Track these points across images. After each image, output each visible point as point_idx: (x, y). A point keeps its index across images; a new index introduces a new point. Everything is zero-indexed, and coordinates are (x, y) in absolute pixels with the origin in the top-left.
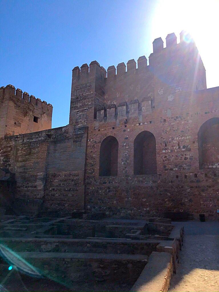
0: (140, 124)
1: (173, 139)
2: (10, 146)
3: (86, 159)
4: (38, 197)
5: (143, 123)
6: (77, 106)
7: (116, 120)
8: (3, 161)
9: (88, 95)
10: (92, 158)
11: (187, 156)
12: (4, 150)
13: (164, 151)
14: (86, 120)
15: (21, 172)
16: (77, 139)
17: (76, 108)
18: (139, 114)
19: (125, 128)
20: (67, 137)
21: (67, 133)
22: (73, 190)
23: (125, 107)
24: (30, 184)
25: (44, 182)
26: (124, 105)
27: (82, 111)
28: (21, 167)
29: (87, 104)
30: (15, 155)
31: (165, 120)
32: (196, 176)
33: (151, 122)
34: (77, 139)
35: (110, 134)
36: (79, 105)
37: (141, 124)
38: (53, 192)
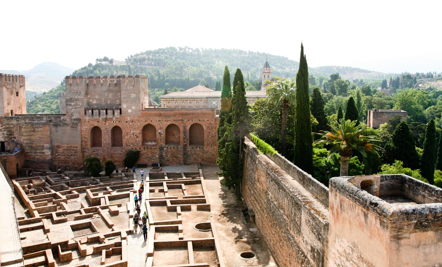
1: (130, 131)
2: (12, 124)
3: (82, 138)
4: (48, 159)
5: (116, 122)
10: (85, 138)
12: (7, 126)
15: (27, 143)
17: (70, 105)
18: (114, 116)
19: (105, 123)
20: (65, 124)
22: (74, 155)
23: (105, 111)
24: (38, 151)
25: (51, 150)
26: (104, 110)
28: (26, 140)
30: (19, 131)
31: (127, 122)
32: (140, 149)
34: (74, 126)
35: (96, 125)
36: (73, 104)
38: (59, 157)
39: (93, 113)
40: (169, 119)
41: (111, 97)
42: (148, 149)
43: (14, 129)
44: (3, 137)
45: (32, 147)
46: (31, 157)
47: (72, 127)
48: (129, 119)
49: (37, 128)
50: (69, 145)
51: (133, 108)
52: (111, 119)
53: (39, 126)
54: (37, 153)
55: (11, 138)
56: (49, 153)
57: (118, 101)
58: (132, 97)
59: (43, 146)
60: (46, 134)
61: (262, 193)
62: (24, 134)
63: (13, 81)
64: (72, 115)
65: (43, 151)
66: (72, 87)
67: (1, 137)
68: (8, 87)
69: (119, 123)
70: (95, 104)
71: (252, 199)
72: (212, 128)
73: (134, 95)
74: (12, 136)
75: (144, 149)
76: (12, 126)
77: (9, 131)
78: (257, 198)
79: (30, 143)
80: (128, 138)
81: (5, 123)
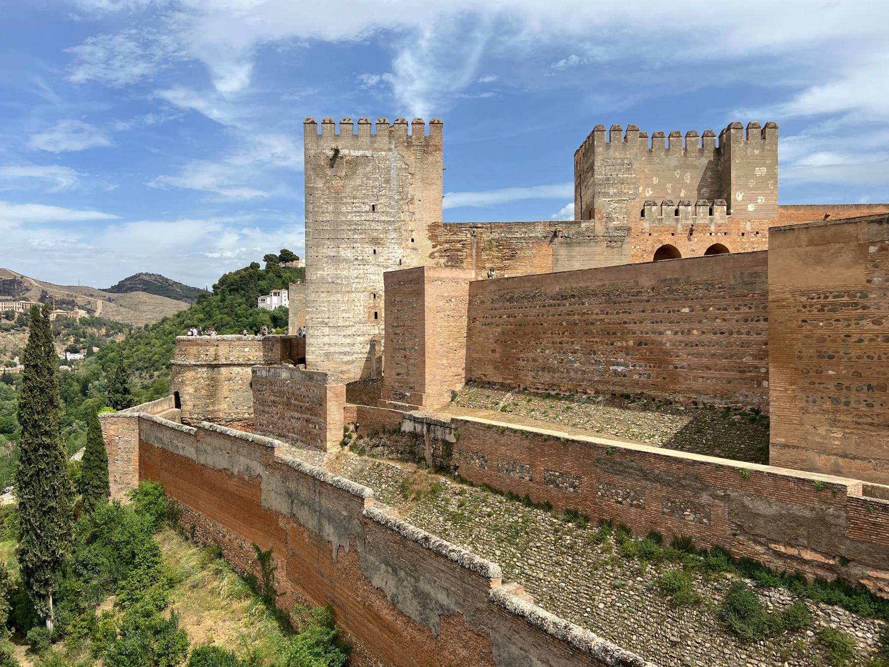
0: (711, 234)
2: (460, 241)
5: (716, 234)
6: (608, 193)
12: (447, 246)
14: (625, 216)
16: (613, 244)
17: (606, 194)
18: (711, 221)
27: (618, 202)
29: (626, 191)
30: (474, 257)
33: (725, 234)
36: (612, 191)
37: (713, 234)
41: (688, 181)
47: (607, 247)
48: (748, 227)
49: (521, 249)
51: (759, 201)
52: (706, 227)
53: (525, 244)
58: (758, 174)
64: (609, 218)
66: (611, 152)
69: (725, 237)
73: (764, 170)
76: (459, 246)
81: (442, 239)
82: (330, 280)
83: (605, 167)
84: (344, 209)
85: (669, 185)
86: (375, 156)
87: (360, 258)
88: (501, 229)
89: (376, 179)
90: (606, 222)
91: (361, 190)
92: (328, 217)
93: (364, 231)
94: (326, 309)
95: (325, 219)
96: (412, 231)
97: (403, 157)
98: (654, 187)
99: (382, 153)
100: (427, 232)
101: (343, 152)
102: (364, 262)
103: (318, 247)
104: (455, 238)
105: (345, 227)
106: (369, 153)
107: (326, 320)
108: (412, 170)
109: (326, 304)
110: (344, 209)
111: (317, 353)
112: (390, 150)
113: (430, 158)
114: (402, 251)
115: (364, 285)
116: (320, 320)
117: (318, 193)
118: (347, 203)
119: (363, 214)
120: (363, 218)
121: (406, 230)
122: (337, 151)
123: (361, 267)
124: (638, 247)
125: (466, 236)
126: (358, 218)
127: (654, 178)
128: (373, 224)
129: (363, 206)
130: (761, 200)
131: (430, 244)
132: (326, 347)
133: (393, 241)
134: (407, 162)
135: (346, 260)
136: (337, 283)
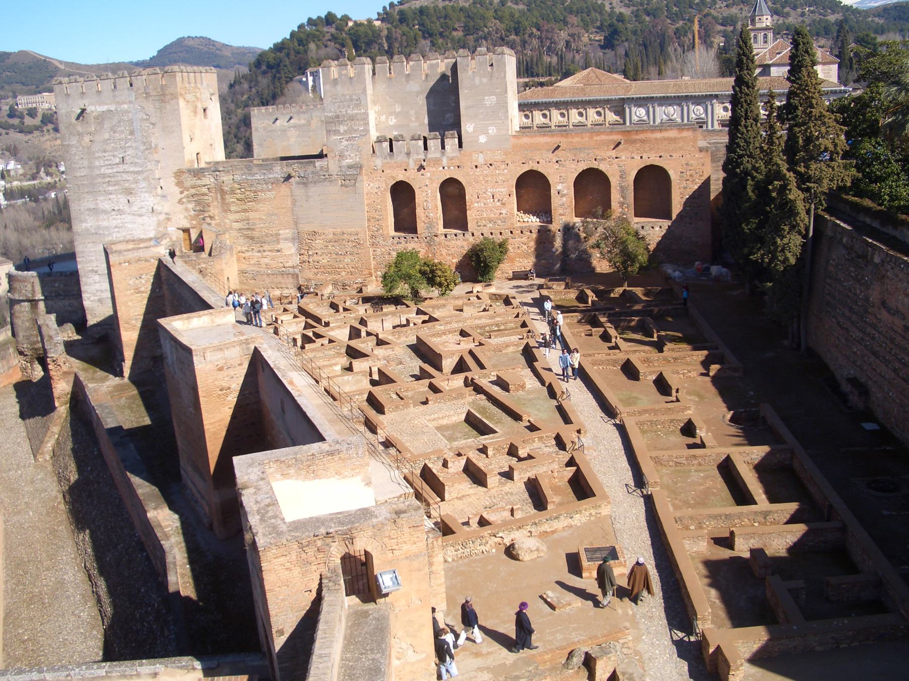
4: (290, 264)
7: (409, 158)
8: (195, 211)
9: (357, 114)
11: (502, 212)
12: (193, 191)
13: (476, 205)
15: (240, 229)
17: (337, 132)
18: (443, 154)
21: (327, 171)
23: (421, 143)
24: (266, 247)
29: (356, 128)
30: (219, 200)
32: (511, 232)
35: (401, 178)
36: (342, 128)
38: (316, 258)
39: (391, 150)
40: (582, 155)
42: (531, 232)
43: (208, 199)
44: (186, 217)
45: (252, 238)
46: (252, 262)
48: (481, 159)
49: (262, 191)
50: (339, 230)
51: (490, 131)
52: (437, 161)
53: (265, 186)
54: (264, 251)
55: (204, 219)
56: (293, 250)
57: (448, 115)
58: (488, 103)
59: (278, 235)
60: (283, 206)
61: (904, 337)
62: (233, 208)
63: (196, 83)
65: (279, 247)
66: (339, 88)
67: (182, 216)
68: (189, 97)
70: (395, 127)
71: (855, 353)
72: (691, 176)
74: (206, 215)
75: (522, 232)
77: (198, 203)
78: (877, 349)
79: (248, 229)
80: (480, 207)
82: (93, 231)
83: (334, 103)
84: (97, 163)
85: (412, 112)
86: (119, 109)
87: (116, 208)
88: (242, 172)
89: (122, 132)
90: (339, 161)
91: (110, 143)
92: (83, 172)
93: (117, 183)
94: (93, 258)
95: (82, 174)
96: (159, 179)
97: (143, 108)
98: (397, 115)
99: (126, 106)
100: (173, 179)
101: (89, 109)
102: (120, 212)
103: (80, 200)
104: (199, 182)
105: (100, 180)
106: (113, 108)
107: (95, 269)
108: (153, 120)
109: (93, 254)
110: (97, 163)
111: (92, 299)
112: (130, 102)
113: (168, 107)
114: (152, 199)
115: (124, 234)
116: (90, 268)
117: (73, 151)
118: (99, 157)
119: (114, 166)
120: (115, 170)
121: (153, 179)
122: (83, 111)
123: (119, 217)
124: (372, 184)
125: (209, 180)
126: (110, 171)
127: (397, 106)
128: (124, 175)
129: (112, 158)
130: (492, 131)
131: (177, 190)
132: (99, 293)
133: (144, 190)
134: (148, 113)
135: (105, 212)
136: (100, 234)
